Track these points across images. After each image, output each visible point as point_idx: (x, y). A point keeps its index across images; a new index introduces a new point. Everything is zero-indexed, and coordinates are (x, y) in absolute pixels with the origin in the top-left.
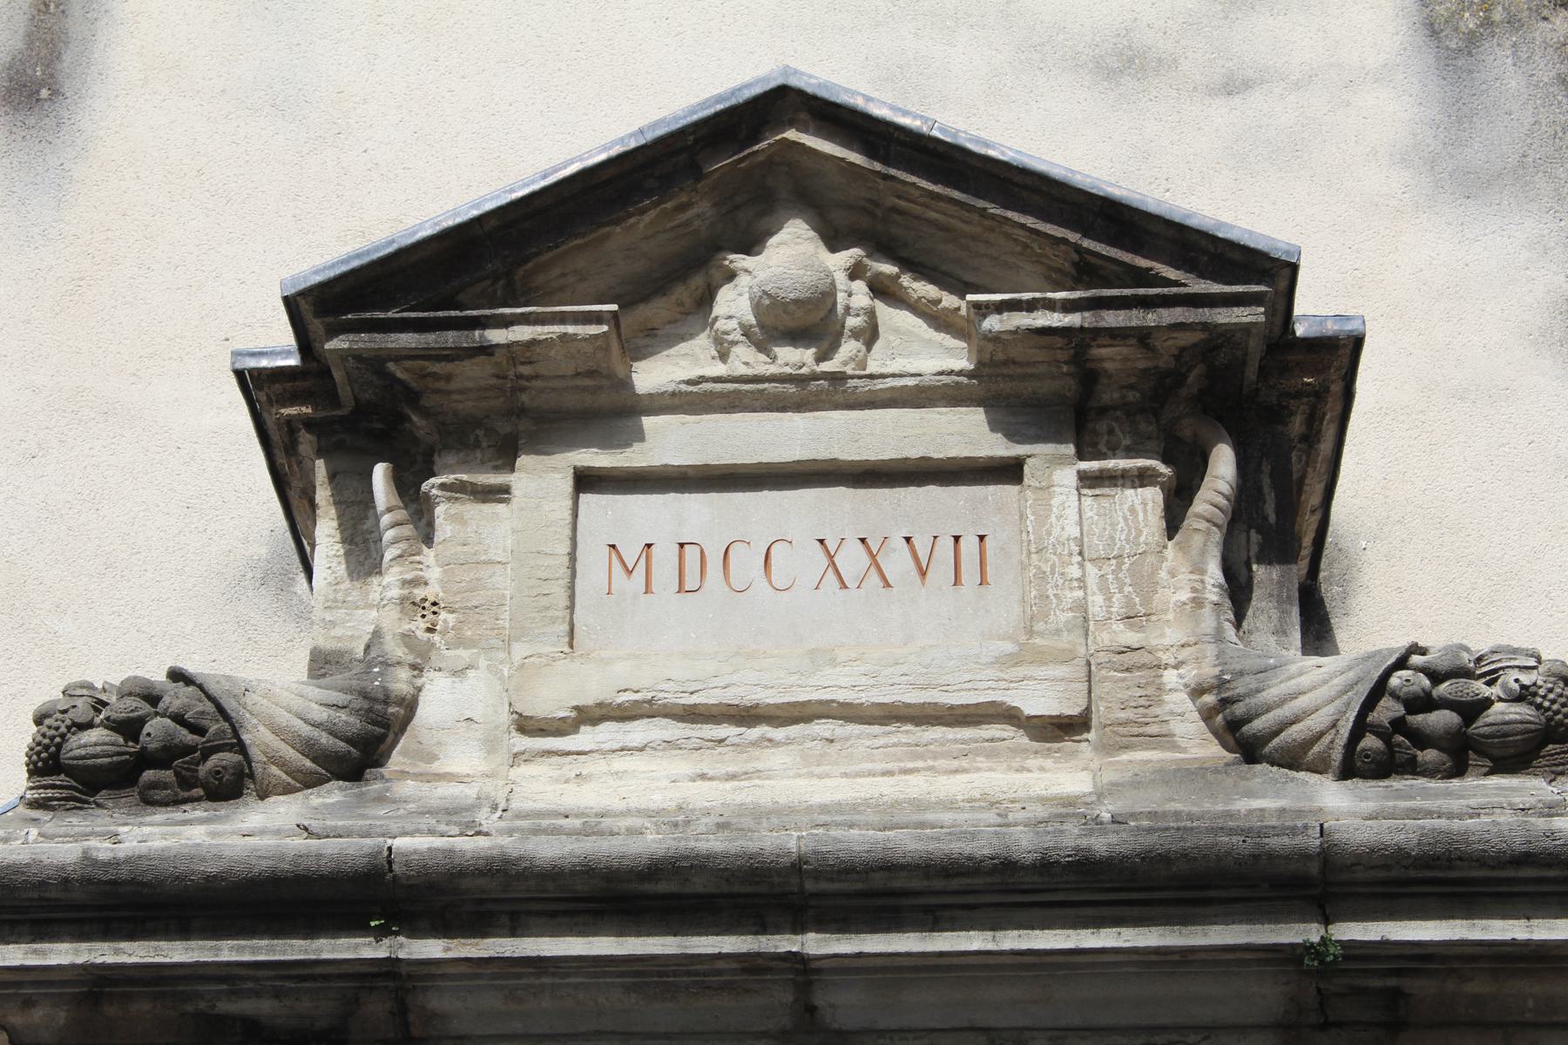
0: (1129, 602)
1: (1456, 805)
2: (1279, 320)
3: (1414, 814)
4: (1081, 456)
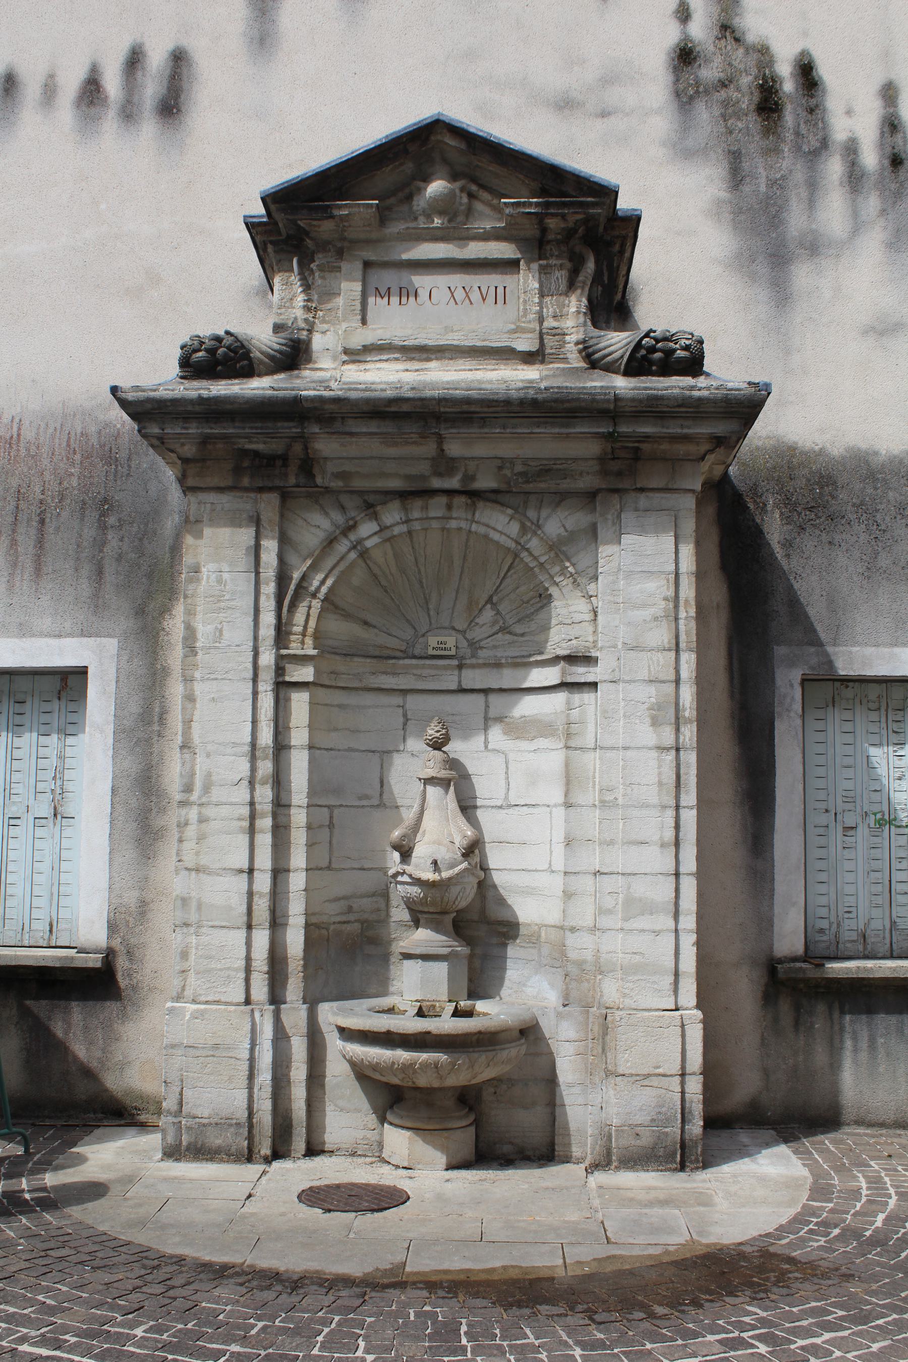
0: (555, 312)
1: (660, 385)
2: (611, 210)
3: (646, 389)
4: (540, 259)
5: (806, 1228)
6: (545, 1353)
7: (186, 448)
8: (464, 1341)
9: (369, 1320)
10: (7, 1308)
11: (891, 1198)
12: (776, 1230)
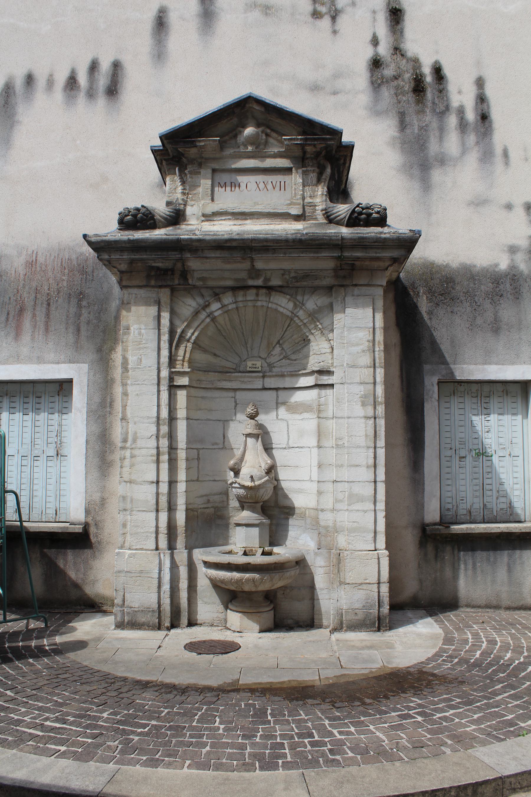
3: (357, 233)
4: (303, 167)
5: (441, 659)
6: (310, 723)
7: (122, 265)
8: (269, 718)
9: (221, 708)
10: (38, 703)
11: (483, 643)
12: (426, 660)
